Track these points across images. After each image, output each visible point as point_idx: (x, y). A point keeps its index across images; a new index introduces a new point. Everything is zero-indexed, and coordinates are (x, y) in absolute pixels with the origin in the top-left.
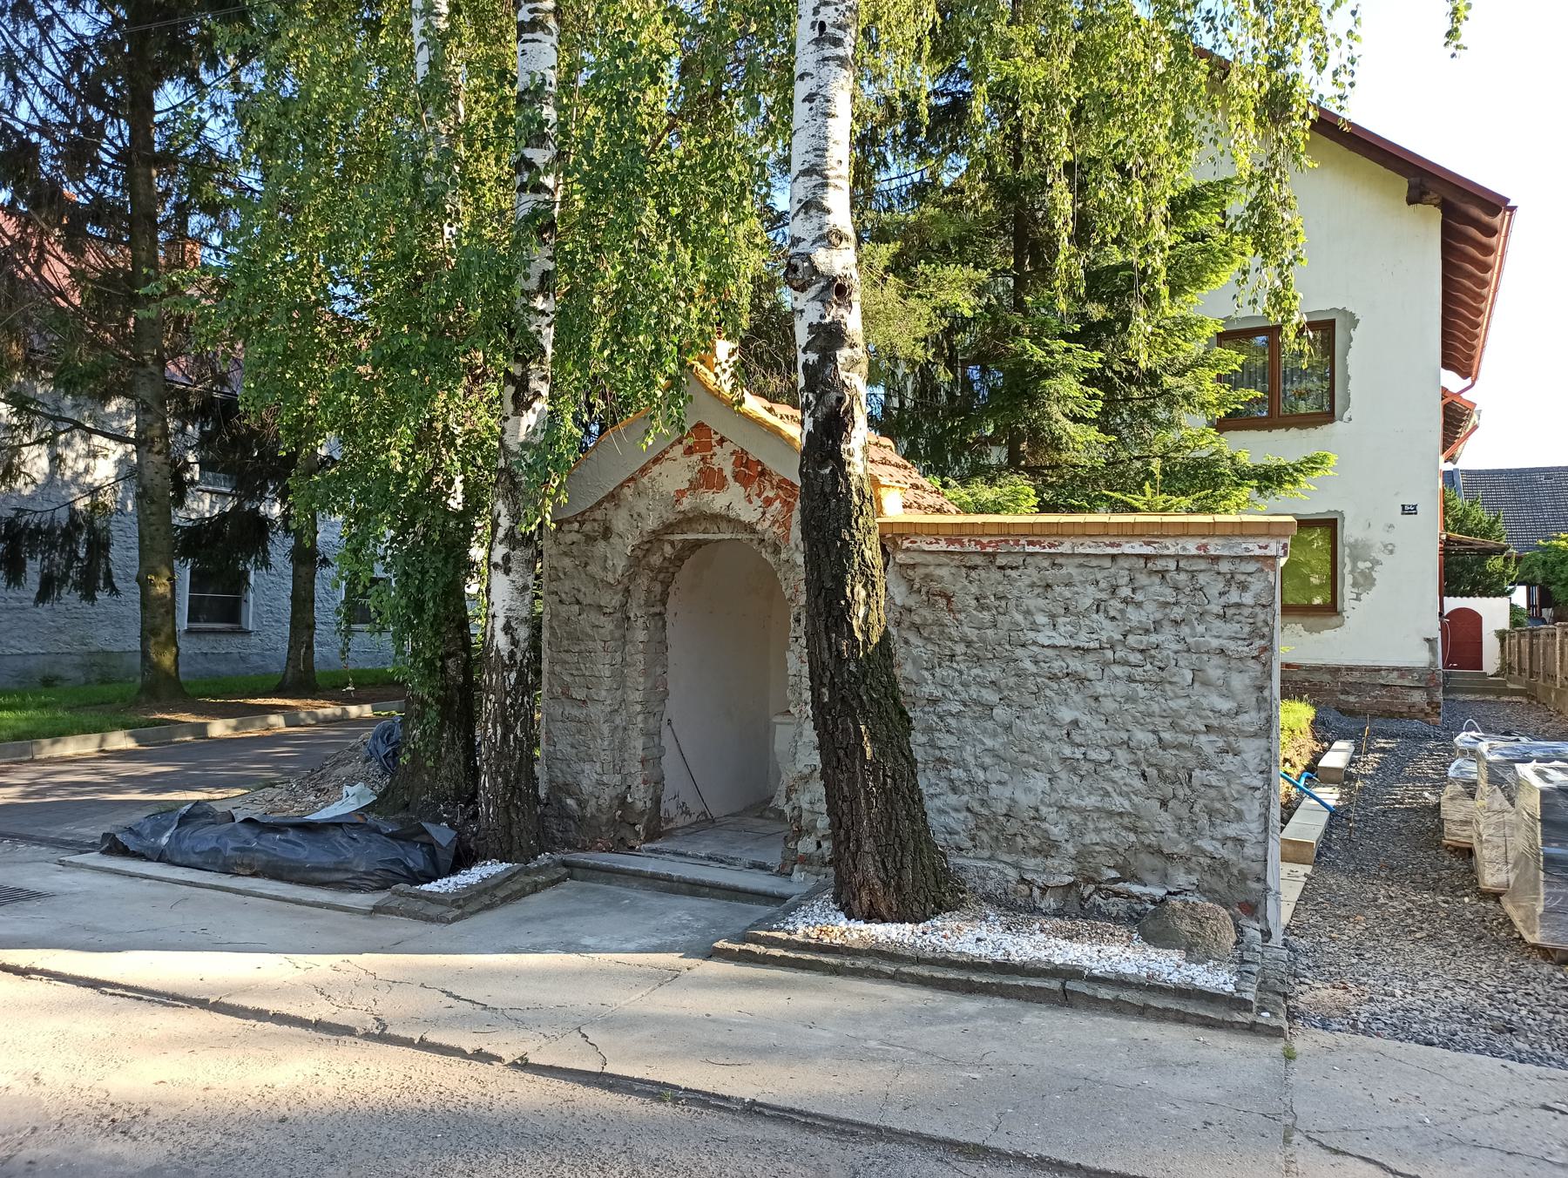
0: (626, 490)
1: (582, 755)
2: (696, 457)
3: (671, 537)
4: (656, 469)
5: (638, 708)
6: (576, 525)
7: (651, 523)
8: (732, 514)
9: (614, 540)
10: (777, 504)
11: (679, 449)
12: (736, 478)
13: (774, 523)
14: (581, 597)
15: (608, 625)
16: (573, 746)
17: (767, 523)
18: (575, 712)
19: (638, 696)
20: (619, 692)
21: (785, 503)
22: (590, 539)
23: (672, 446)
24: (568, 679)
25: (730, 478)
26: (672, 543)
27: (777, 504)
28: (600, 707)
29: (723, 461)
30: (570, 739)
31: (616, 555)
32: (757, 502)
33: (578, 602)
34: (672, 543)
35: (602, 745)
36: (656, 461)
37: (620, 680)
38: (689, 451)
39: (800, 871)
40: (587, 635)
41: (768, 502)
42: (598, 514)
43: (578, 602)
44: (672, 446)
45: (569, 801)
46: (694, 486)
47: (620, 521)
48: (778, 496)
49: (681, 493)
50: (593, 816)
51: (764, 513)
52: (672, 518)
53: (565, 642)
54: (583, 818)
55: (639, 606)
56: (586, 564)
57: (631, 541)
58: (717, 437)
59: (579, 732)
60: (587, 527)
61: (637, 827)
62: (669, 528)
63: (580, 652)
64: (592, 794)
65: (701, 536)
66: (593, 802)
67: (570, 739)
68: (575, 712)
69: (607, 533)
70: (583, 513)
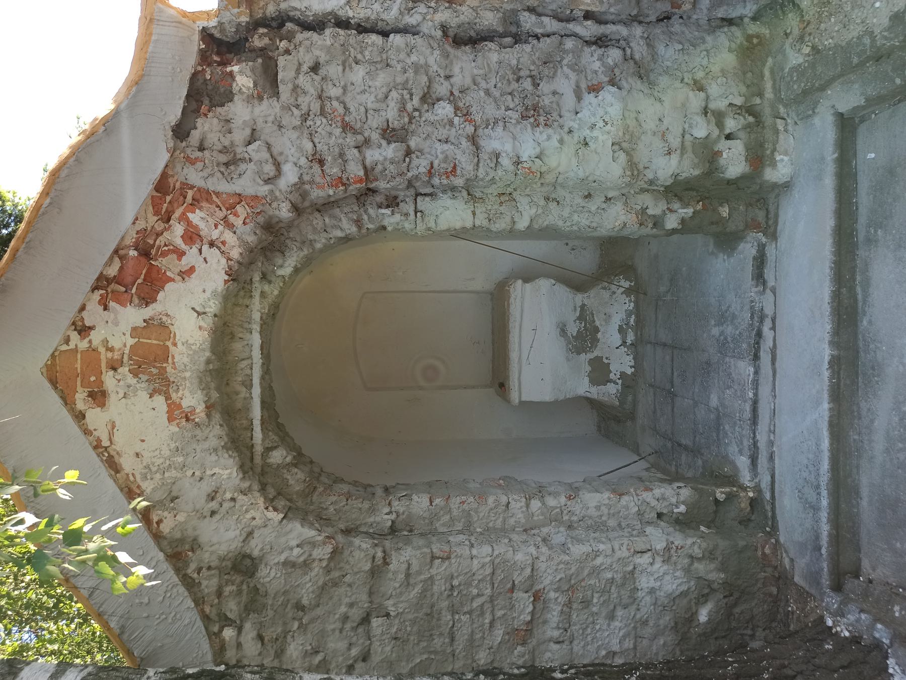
0: (165, 528)
1: (625, 593)
2: (109, 380)
3: (259, 449)
4: (128, 464)
5: (536, 504)
6: (228, 633)
7: (226, 471)
8: (213, 307)
9: (255, 547)
10: (196, 217)
11: (96, 418)
12: (147, 299)
13: (230, 226)
14: (356, 614)
15: (405, 556)
16: (611, 617)
17: (229, 236)
18: (554, 616)
19: (517, 504)
20: (515, 537)
21: (195, 204)
22: (254, 602)
23: (87, 432)
24: (499, 633)
25: (148, 312)
26: (268, 450)
27: (196, 217)
28: (542, 566)
29: (118, 327)
30: (601, 622)
31: (282, 539)
32: (192, 257)
33: (366, 620)
34: (268, 450)
35: (610, 553)
36: (113, 465)
37: (491, 534)
38: (99, 396)
39: (774, 164)
40: (424, 590)
41: (192, 236)
42: (209, 584)
43: (366, 620)
44: (87, 432)
45: (703, 616)
46: (162, 386)
47: (220, 538)
48: (183, 218)
49: (174, 412)
50: (723, 568)
51: (212, 244)
52: (215, 433)
53: (438, 642)
54: (729, 588)
55: (372, 510)
56: (300, 607)
57: (258, 512)
58: (74, 336)
59: (586, 603)
60: (232, 608)
61: (721, 497)
62: (237, 443)
63: (454, 611)
64: (687, 571)
65: (257, 391)
66: (700, 568)
67: (601, 622)
68: (554, 616)
69: (243, 565)
70: (206, 618)
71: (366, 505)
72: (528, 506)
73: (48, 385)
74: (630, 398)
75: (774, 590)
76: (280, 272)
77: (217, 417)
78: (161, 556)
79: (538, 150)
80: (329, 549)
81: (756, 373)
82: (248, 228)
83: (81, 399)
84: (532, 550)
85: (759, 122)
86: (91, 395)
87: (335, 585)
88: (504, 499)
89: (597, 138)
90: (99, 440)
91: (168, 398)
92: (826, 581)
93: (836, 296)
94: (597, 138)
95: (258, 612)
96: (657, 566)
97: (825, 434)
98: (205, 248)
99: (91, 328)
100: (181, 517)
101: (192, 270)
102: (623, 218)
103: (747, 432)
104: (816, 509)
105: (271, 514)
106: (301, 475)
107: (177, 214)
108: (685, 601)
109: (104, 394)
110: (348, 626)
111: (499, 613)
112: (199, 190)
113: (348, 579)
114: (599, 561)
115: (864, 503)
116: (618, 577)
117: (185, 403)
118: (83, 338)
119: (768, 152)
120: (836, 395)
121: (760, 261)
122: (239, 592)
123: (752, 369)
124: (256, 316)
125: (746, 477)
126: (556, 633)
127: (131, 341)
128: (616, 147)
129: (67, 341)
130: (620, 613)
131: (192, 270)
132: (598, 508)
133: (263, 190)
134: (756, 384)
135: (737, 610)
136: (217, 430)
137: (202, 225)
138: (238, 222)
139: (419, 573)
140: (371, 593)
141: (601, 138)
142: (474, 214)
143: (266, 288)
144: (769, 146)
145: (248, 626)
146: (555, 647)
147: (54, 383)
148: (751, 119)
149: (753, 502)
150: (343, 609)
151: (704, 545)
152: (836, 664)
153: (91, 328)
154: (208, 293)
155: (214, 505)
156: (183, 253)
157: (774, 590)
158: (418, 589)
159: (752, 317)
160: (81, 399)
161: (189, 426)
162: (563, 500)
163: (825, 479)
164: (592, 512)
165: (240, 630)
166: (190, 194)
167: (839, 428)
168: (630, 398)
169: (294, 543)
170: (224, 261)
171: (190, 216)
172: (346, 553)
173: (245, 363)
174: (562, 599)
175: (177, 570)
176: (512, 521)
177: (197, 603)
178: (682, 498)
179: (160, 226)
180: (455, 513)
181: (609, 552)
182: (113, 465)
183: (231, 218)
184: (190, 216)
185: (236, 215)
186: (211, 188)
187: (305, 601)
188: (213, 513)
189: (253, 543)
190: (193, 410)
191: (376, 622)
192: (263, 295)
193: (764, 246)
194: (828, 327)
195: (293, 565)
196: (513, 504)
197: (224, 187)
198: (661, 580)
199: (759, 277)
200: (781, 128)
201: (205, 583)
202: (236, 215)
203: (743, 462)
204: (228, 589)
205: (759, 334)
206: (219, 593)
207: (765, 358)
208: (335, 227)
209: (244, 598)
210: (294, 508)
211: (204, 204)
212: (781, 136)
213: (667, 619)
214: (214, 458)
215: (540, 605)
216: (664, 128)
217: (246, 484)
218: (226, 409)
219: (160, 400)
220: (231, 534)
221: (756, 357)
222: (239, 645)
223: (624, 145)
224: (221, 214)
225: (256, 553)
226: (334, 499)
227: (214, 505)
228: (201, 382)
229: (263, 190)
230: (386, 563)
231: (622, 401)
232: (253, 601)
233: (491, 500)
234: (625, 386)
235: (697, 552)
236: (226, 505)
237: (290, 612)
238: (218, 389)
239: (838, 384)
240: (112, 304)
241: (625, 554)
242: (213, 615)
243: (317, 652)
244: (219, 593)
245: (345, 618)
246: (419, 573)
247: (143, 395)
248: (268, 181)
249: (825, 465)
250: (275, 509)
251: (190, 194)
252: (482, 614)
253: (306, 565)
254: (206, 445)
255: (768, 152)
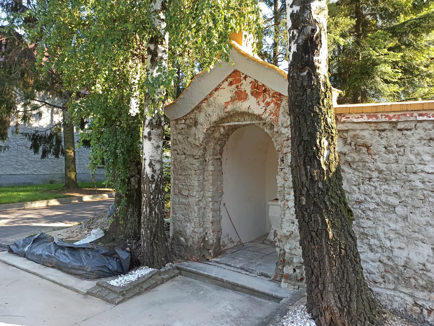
0: (203, 104)
1: (186, 219)
2: (234, 86)
3: (224, 125)
4: (216, 93)
5: (210, 199)
6: (183, 121)
7: (214, 118)
8: (250, 111)
9: (199, 126)
10: (272, 105)
11: (226, 83)
12: (252, 94)
13: (270, 114)
14: (186, 151)
15: (197, 163)
16: (183, 215)
17: (267, 114)
18: (184, 201)
19: (210, 194)
20: (202, 193)
21: (276, 104)
22: (189, 127)
23: (223, 82)
24: (181, 186)
25: (249, 94)
26: (224, 127)
27: (272, 105)
28: (193, 198)
29: (246, 86)
30: (182, 212)
31: (200, 133)
32: (262, 104)
33: (185, 154)
34: (224, 127)
35: (194, 215)
36: (216, 90)
38: (231, 84)
39: (285, 282)
40: (188, 168)
41: (268, 104)
42: (192, 116)
43: (185, 154)
44: (223, 82)
45: (182, 239)
46: (233, 100)
47: (201, 118)
48: (272, 101)
49: (227, 103)
50: (191, 246)
51: (266, 110)
52: (223, 115)
53: (180, 171)
54: (187, 246)
55: (210, 155)
56: (188, 138)
57: (206, 126)
58: (243, 76)
59: (185, 209)
60: (188, 122)
61: (210, 251)
62: (222, 120)
63: (185, 175)
64: (190, 236)
65: (236, 123)
66: (191, 240)
67: (182, 212)
68: (184, 201)
69: (196, 123)
70: (186, 115)
71: (211, 154)
72: (209, 197)
73: (232, 71)
74: (268, 243)
75: (186, 258)
76: (265, 128)
77: (227, 114)
78: (197, 104)
79: (290, 207)
80: (198, 145)
81: (238, 268)
82: (269, 119)
83: (230, 80)
84: (197, 197)
85: (298, 281)
86: (231, 82)
87: (191, 146)
88: (211, 191)
89: (293, 226)
90: (221, 85)
91: (230, 101)
92: (179, 266)
93: (238, 285)
94: (293, 226)
95: (187, 128)
96: (192, 228)
97: (208, 274)
98: (264, 108)
99: (245, 80)
100: (205, 108)
101: (259, 105)
102: (279, 234)
103: (225, 262)
104: (194, 268)
105: (205, 130)
106: (218, 136)
107: (274, 99)
108: (185, 234)
109: (232, 85)
110: (183, 149)
111: (184, 186)
112: (280, 105)
113: (192, 149)
114: (193, 213)
115: (193, 280)
116: (190, 218)
117: (229, 106)
118: (243, 78)
119: (288, 281)
120: (215, 279)
121: (266, 276)
122: (191, 123)
123: (238, 267)
124: (254, 122)
125: (214, 259)
126: (180, 201)
127: (243, 90)
128: (291, 232)
129: (243, 74)
130: (183, 217)
131: (259, 105)
132: (208, 216)
133: (280, 123)
134: (235, 267)
135: (182, 248)
136: (223, 115)
137: (270, 106)
138: (271, 117)
139: (193, 167)
140: (189, 155)
141: (294, 227)
142: (281, 187)
143: (261, 124)
144: (290, 282)
145: (185, 125)
146: (178, 200)
147: (234, 72)
148: (299, 278)
149: (208, 260)
150: (186, 148)
151: (196, 242)
152: (158, 258)
153: (245, 80)
154: (253, 110)
155: (208, 115)
156: (263, 102)
157: (186, 258)
158: (190, 167)
159: (251, 270)
160: (230, 80)
161: (224, 108)
162: (211, 207)
163: (199, 271)
164: (207, 215)
165: (184, 124)
166: (279, 102)
167: (208, 277)
168: (268, 243)
169: (199, 136)
170: (261, 113)
171: (273, 103)
172: (198, 149)
173: (243, 119)
174: (186, 203)
175: (195, 108)
176: (206, 193)
177: (189, 113)
178: (210, 240)
179: (271, 94)
180: (209, 177)
181: (195, 216)
182: (216, 90)
183: (272, 115)
184: (273, 103)
185: (273, 116)
186: (280, 108)
187: (188, 139)
188: (206, 115)
189: (200, 126)
190: (227, 108)
191: (184, 156)
192: (260, 123)
193: (270, 278)
194: (231, 281)
195: (195, 136)
196: (210, 193)
197: (280, 112)
198: (189, 228)
199: (262, 275)
200: (295, 287)
201: (192, 115)
202: (273, 116)
203: (218, 260)
204: (191, 120)
205: (247, 271)
206: (191, 118)
207: (239, 271)
208: (277, 144)
209: (190, 124)
210: (209, 135)
211: (276, 107)
212: (293, 287)
213: (182, 229)
214: (217, 115)
215: (186, 197)
216: (297, 249)
217: (212, 123)
218: (231, 116)
219: (230, 99)
220: (201, 120)
221: (241, 269)
222: (181, 124)
223: (292, 235)
224: (273, 111)
225: (198, 127)
226: (213, 145)
227: (208, 115)
228: (234, 110)
229: (280, 123)
230: (195, 159)
231: (268, 240)
232: (190, 126)
233: (211, 187)
234: (272, 242)
235: (194, 240)
236: (207, 118)
237: (186, 135)
238: (233, 114)
239: (218, 280)
240: (251, 84)
241: (195, 221)
242: (187, 117)
243: (179, 142)
244: (191, 118)
245: (185, 149)
246: (193, 167)
247: (231, 96)
248: (282, 124)
249: (201, 272)
250: (207, 131)
251: (279, 102)
252: (185, 182)
253: (195, 139)
254: (220, 113)
255: (288, 281)
